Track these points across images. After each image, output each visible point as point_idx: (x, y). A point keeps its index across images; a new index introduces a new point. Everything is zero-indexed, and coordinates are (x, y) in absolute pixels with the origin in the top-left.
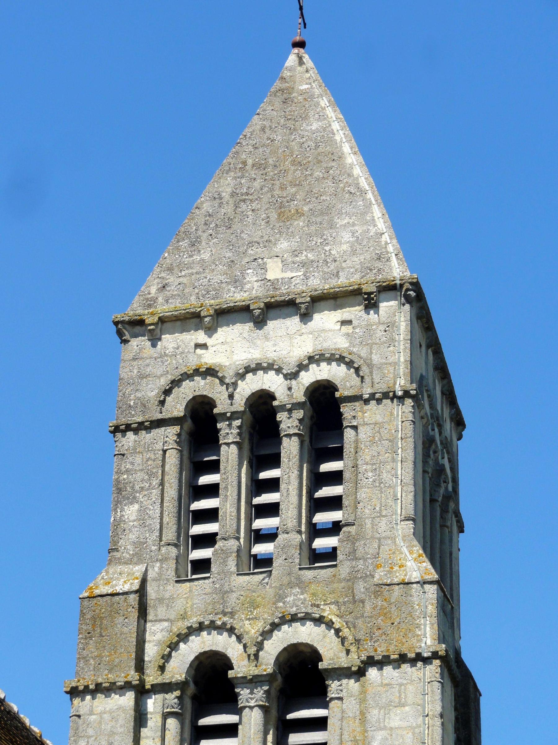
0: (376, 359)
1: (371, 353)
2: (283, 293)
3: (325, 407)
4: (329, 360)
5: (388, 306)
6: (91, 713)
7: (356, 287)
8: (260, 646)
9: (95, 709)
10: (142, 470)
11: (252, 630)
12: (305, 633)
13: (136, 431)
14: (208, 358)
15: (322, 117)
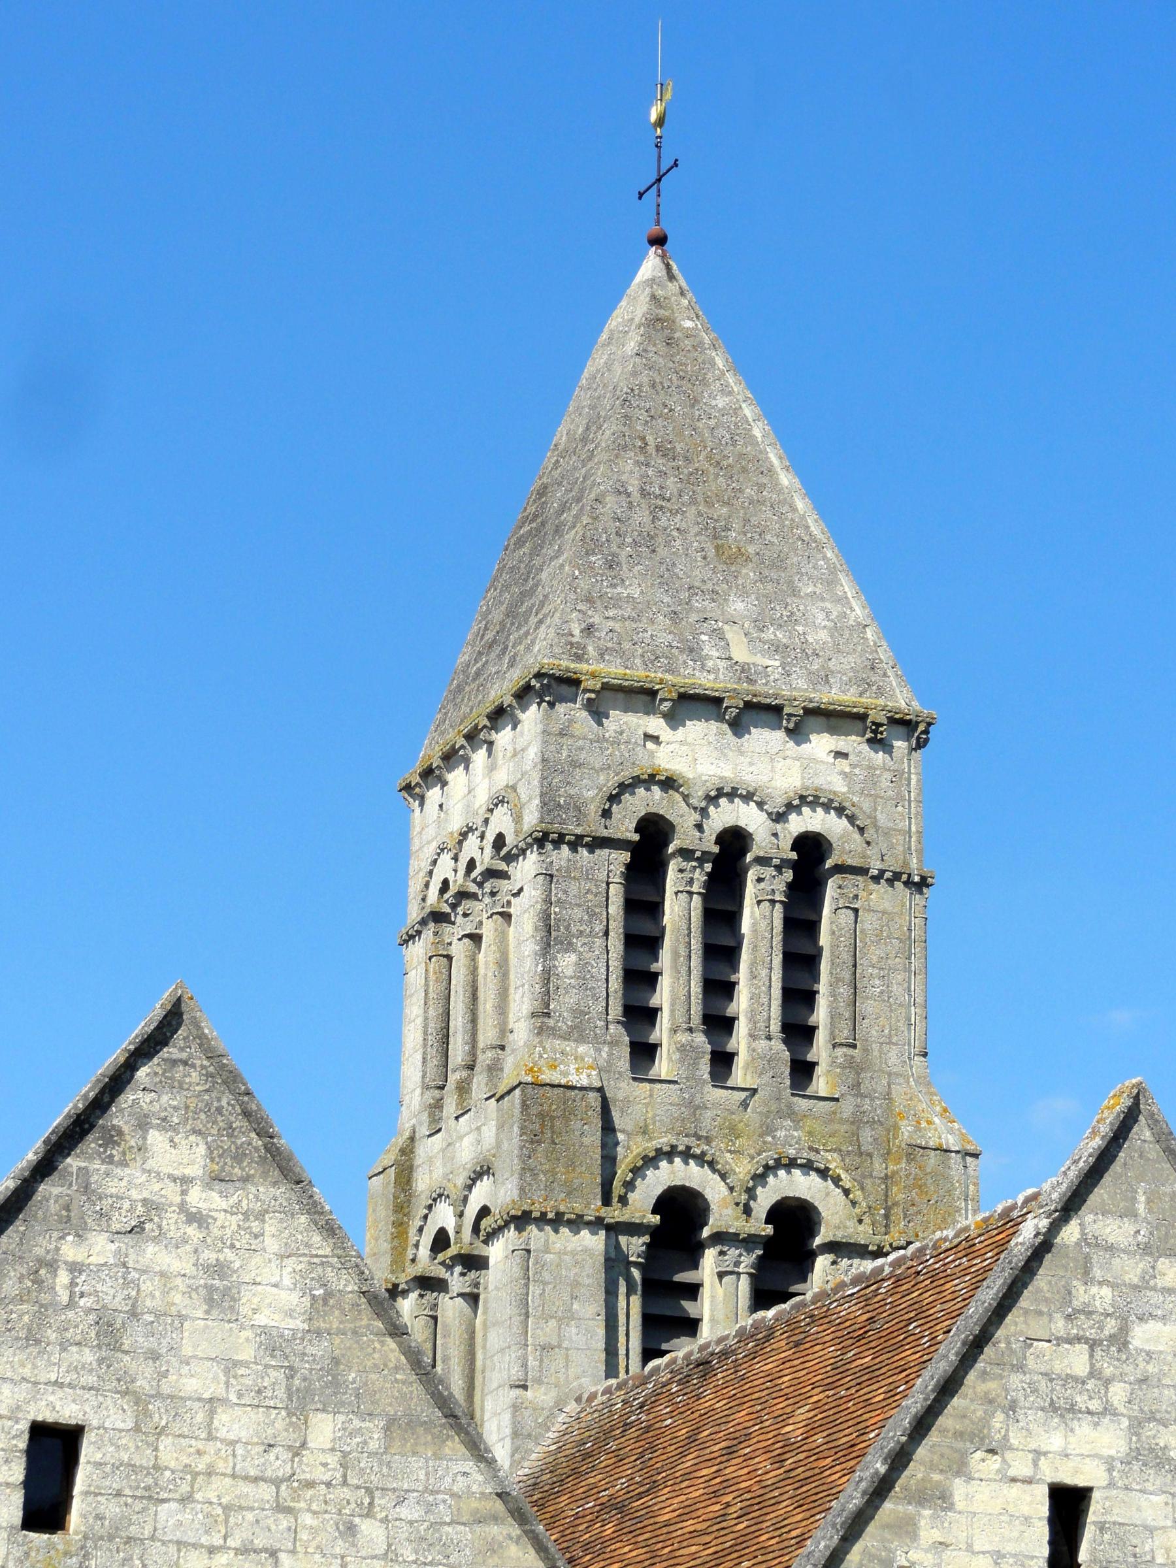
0: (882, 818)
1: (875, 810)
4: (827, 807)
6: (547, 1250)
7: (862, 710)
8: (751, 1192)
9: (551, 1246)
10: (579, 905)
11: (743, 1169)
13: (574, 846)
15: (726, 391)
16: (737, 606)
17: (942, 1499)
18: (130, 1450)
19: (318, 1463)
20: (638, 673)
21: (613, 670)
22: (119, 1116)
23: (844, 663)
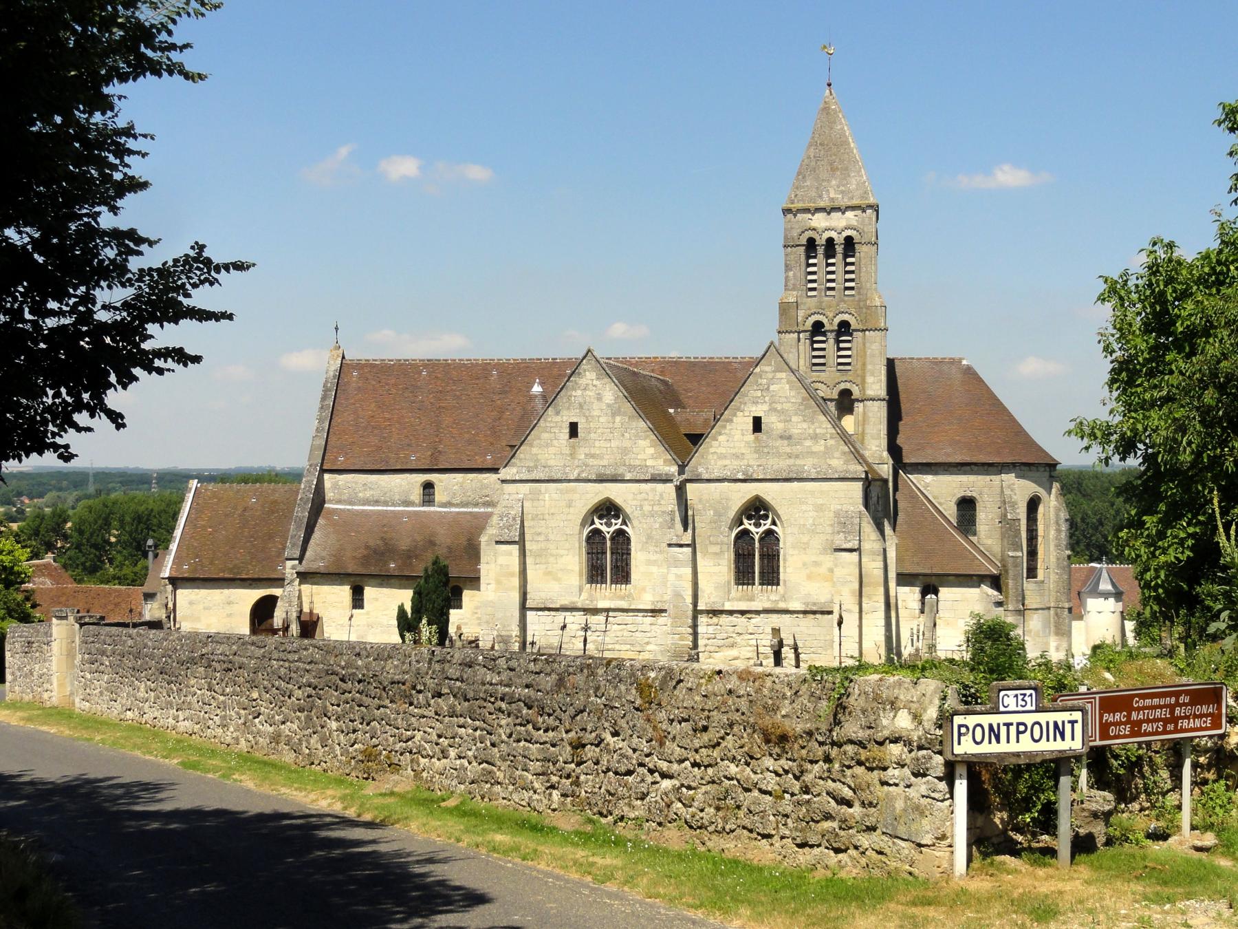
2: (836, 204)
3: (849, 242)
11: (831, 315)
12: (846, 317)
14: (814, 224)
16: (834, 182)
17: (731, 421)
19: (618, 424)
20: (807, 205)
21: (800, 205)
22: (581, 370)
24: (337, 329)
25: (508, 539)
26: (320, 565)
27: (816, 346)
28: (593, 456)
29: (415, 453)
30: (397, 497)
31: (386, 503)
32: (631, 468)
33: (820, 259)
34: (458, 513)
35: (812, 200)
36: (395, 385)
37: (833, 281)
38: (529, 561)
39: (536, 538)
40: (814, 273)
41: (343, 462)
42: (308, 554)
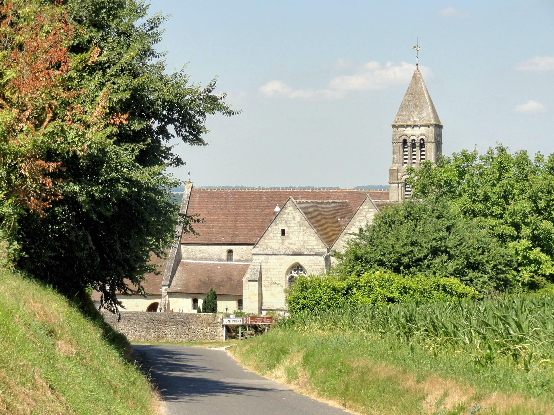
2: (416, 124)
5: (431, 127)
16: (416, 113)
18: (288, 230)
21: (400, 124)
23: (426, 118)
24: (189, 173)
25: (254, 279)
26: (178, 289)
27: (407, 189)
28: (291, 244)
29: (224, 235)
30: (215, 257)
31: (210, 260)
32: (307, 249)
33: (409, 149)
34: (244, 265)
35: (405, 121)
36: (217, 202)
37: (415, 159)
38: (264, 289)
39: (267, 279)
40: (407, 155)
41: (190, 240)
42: (173, 283)
